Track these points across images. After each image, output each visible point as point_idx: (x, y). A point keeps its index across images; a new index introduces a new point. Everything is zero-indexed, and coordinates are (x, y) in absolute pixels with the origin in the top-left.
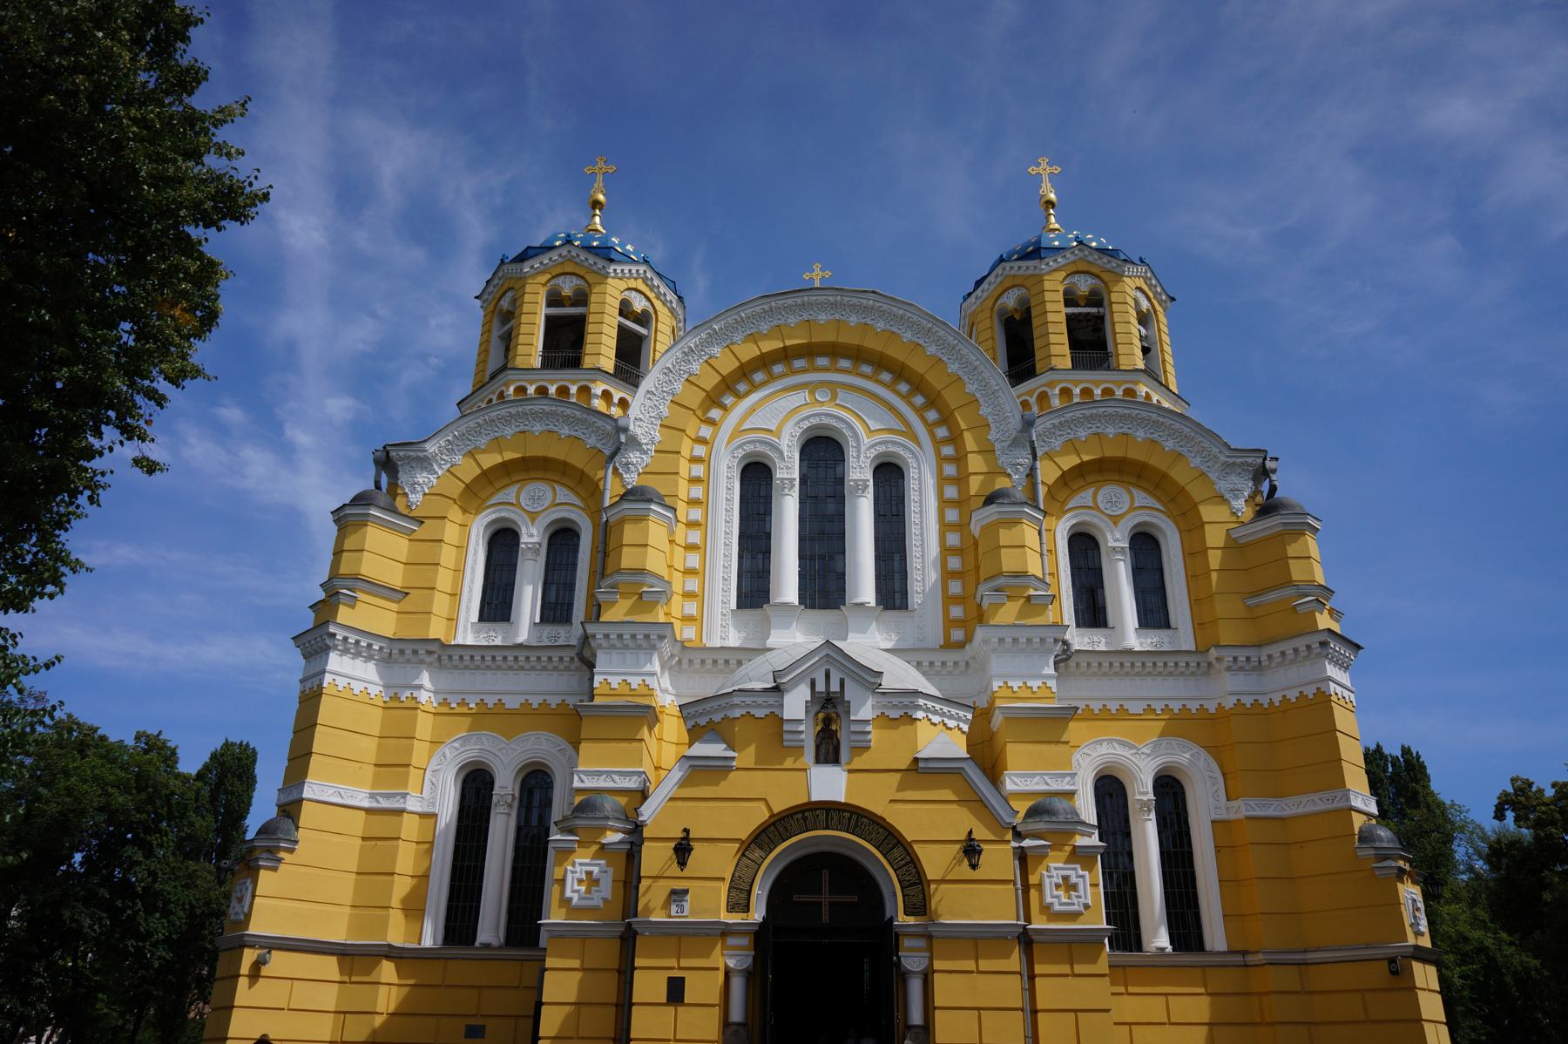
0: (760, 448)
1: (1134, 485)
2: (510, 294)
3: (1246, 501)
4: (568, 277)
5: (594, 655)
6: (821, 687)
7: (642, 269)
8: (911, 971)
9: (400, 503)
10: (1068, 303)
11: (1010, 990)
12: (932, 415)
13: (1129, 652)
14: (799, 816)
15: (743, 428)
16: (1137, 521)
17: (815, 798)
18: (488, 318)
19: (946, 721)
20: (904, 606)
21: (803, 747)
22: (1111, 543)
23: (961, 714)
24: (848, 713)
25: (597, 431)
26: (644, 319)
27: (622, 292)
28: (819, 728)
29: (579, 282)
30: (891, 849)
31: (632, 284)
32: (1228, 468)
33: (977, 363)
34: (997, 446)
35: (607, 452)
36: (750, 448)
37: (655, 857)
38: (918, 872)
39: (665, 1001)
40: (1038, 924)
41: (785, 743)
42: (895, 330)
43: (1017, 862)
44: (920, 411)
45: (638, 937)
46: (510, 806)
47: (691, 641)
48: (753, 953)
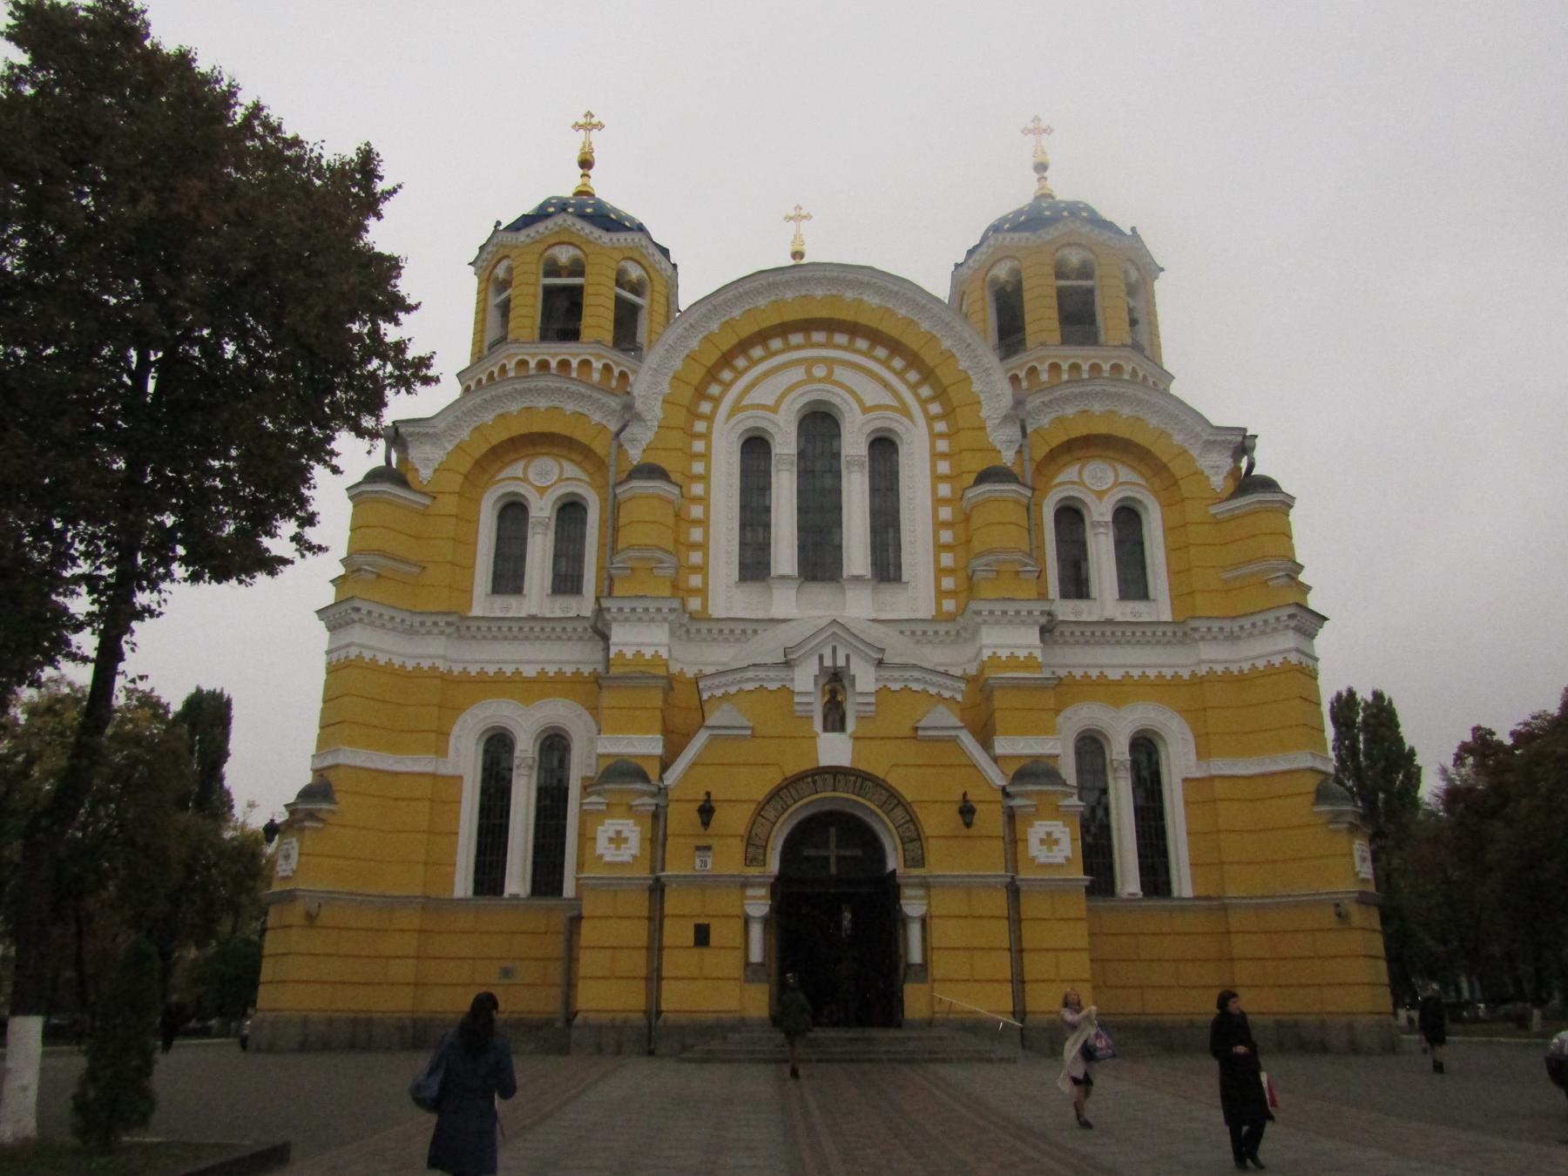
1: (1117, 460)
2: (505, 263)
3: (1225, 478)
5: (608, 625)
6: (828, 662)
8: (911, 917)
9: (410, 477)
10: (1060, 275)
11: (1000, 933)
12: (925, 391)
13: (1109, 622)
14: (810, 780)
15: (746, 402)
16: (1121, 495)
17: (825, 760)
18: (483, 285)
19: (943, 692)
20: (897, 578)
21: (812, 717)
22: (1096, 518)
23: (957, 684)
24: (853, 684)
25: (602, 408)
26: (637, 289)
27: (618, 262)
28: (826, 699)
30: (893, 809)
31: (626, 255)
32: (1209, 445)
33: (969, 341)
34: (989, 424)
35: (614, 428)
36: (750, 424)
37: (682, 817)
38: (917, 830)
39: (691, 941)
43: (1006, 818)
44: (913, 388)
45: (667, 891)
46: (531, 768)
47: (696, 612)
48: (770, 902)
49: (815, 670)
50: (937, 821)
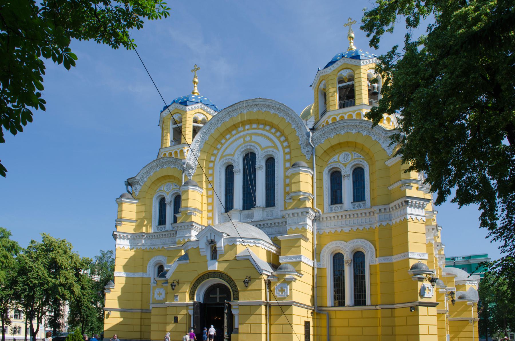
0: (230, 161)
4: (176, 114)
6: (209, 238)
7: (199, 105)
15: (224, 155)
29: (179, 115)
31: (197, 111)
40: (273, 301)
41: (201, 255)
42: (268, 110)
44: (279, 138)
49: (206, 241)
50: (240, 286)
